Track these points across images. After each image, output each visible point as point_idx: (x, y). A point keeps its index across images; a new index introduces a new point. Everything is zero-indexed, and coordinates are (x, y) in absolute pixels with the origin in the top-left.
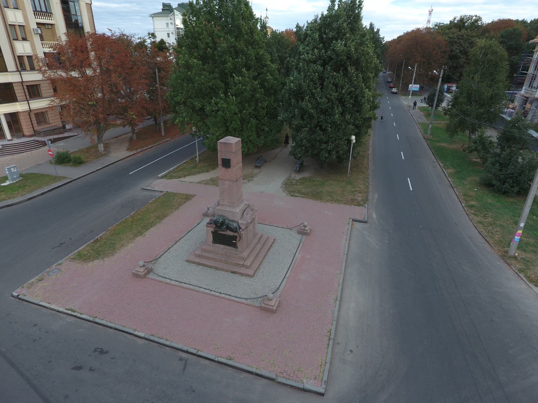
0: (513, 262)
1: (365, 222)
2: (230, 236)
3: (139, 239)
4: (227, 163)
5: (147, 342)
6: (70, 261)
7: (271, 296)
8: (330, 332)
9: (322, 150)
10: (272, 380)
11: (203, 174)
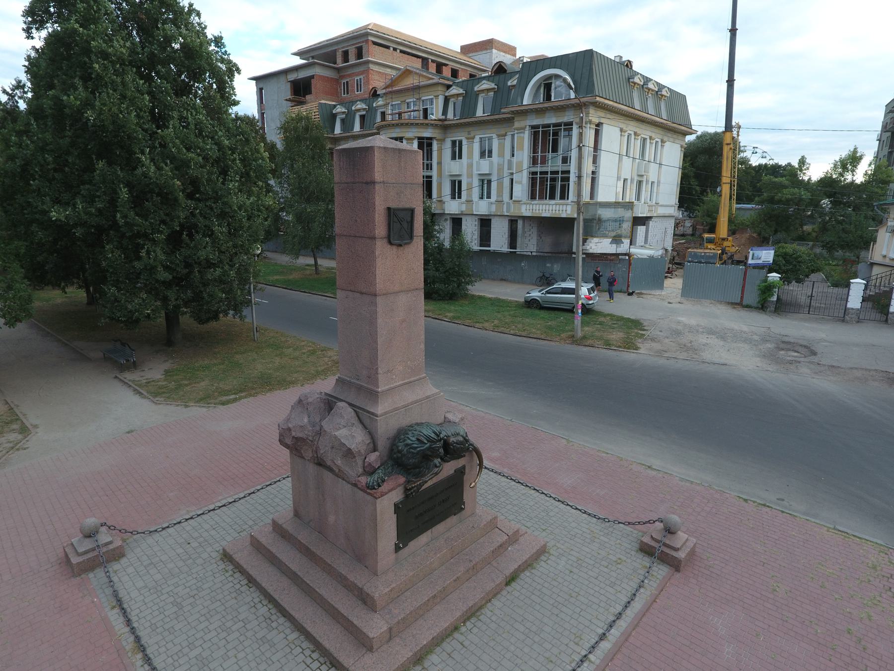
0: (589, 342)
2: (449, 479)
7: (675, 518)
8: (746, 500)
9: (205, 285)
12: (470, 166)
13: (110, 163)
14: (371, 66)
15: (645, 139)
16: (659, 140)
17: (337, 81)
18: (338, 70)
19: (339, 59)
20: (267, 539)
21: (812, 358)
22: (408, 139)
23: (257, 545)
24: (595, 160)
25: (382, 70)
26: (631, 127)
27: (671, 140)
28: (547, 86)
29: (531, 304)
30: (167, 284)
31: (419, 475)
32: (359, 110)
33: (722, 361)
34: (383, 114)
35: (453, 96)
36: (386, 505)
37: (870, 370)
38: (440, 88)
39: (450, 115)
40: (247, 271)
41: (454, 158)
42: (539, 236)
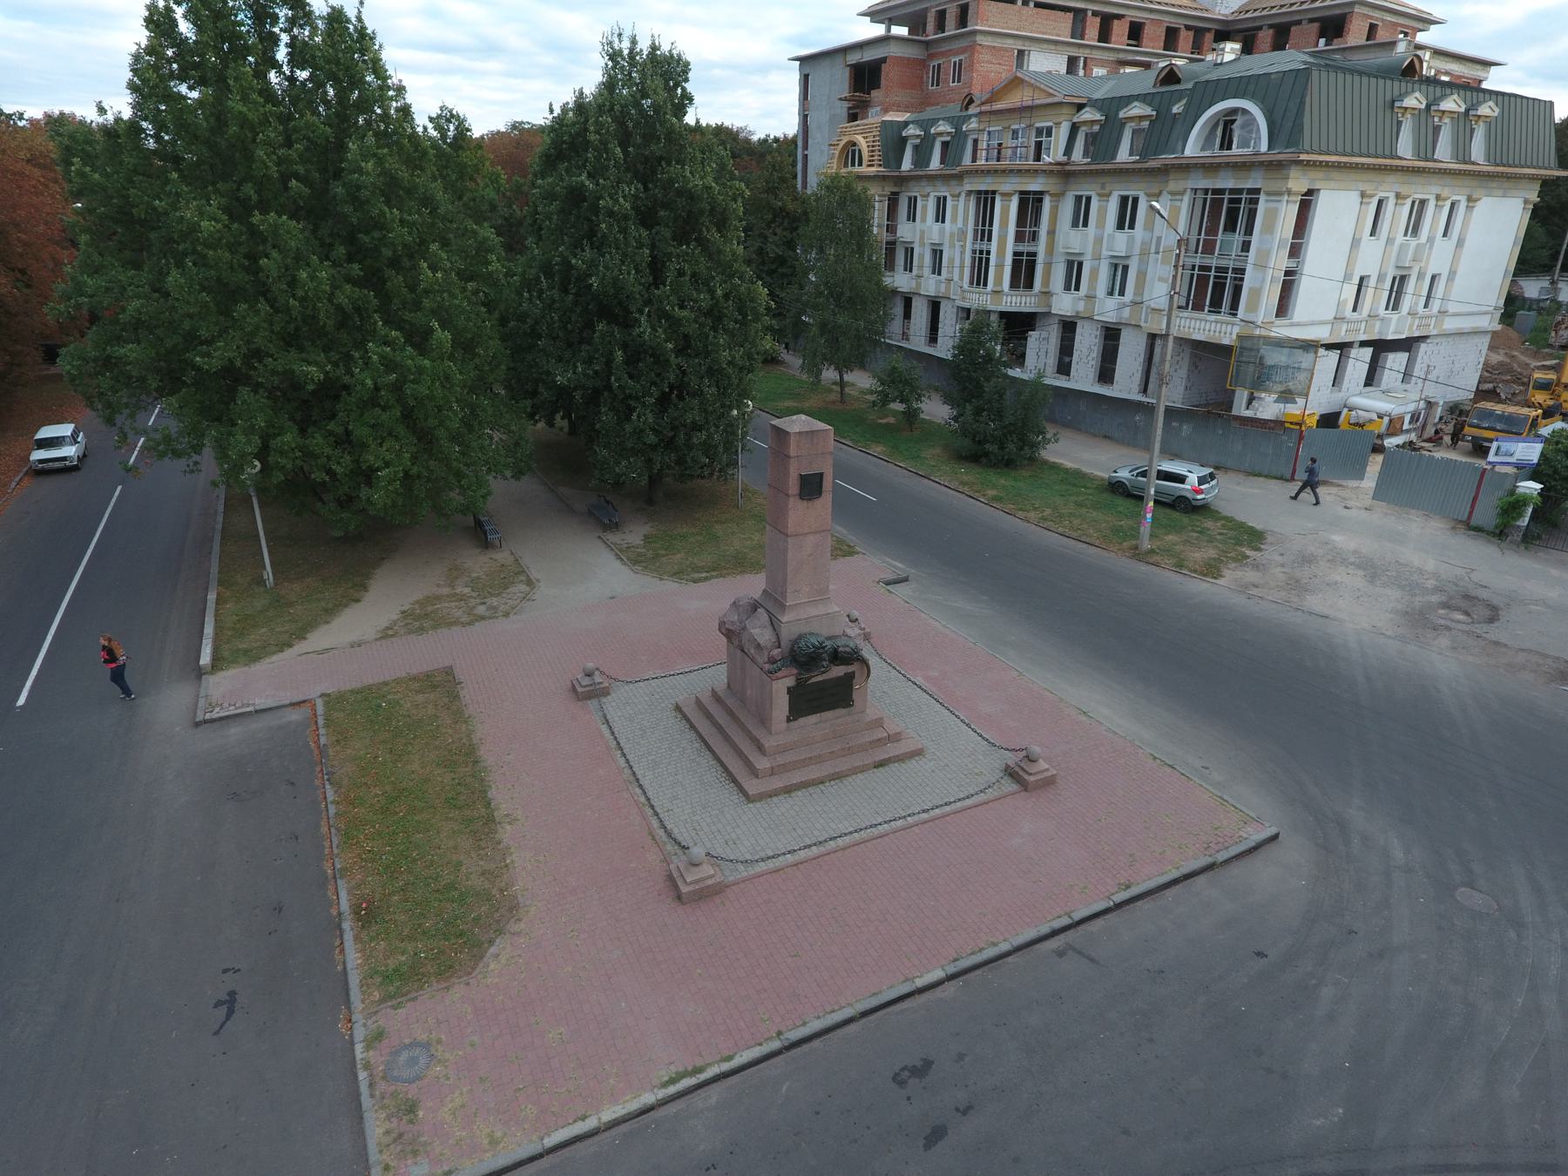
1: (905, 580)
3: (506, 833)
4: (811, 486)
5: (959, 982)
6: (394, 1008)
7: (1036, 749)
9: (690, 448)
10: (1211, 867)
11: (347, 610)
12: (1099, 240)
13: (609, 323)
14: (979, 39)
15: (1423, 202)
16: (1463, 199)
17: (922, 64)
18: (927, 44)
19: (930, 26)
20: (706, 700)
21: (1479, 629)
22: (1003, 195)
23: (698, 702)
24: (1295, 251)
25: (998, 43)
26: (1387, 189)
27: (1500, 192)
28: (1228, 125)
29: (1116, 487)
30: (654, 447)
31: (808, 671)
32: (941, 134)
33: (1326, 611)
34: (976, 141)
35: (1085, 123)
36: (781, 687)
37: (1547, 656)
38: (1065, 110)
39: (1078, 155)
40: (734, 433)
41: (1075, 224)
42: (1194, 366)
